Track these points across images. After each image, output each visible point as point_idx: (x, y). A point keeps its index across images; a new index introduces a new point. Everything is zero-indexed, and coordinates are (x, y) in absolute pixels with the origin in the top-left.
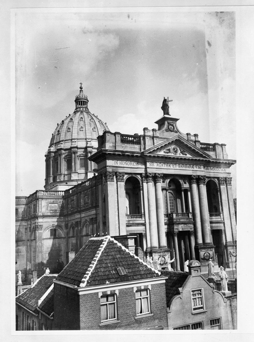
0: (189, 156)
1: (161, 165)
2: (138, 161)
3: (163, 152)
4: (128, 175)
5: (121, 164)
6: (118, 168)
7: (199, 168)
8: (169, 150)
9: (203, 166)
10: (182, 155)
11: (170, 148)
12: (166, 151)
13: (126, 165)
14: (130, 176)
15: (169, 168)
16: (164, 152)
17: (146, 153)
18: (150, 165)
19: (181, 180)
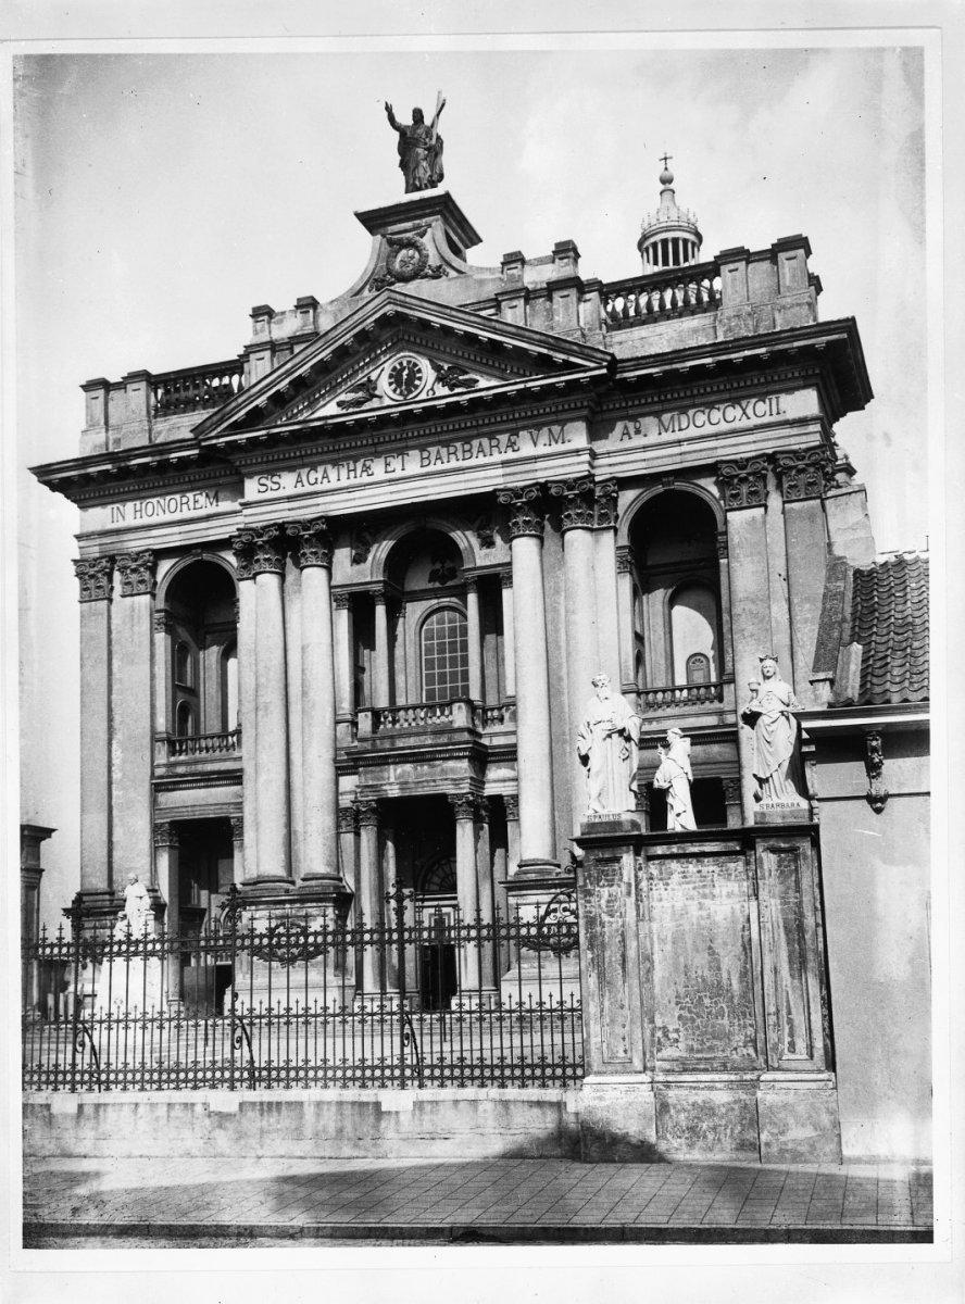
0: (486, 384)
1: (319, 475)
2: (215, 486)
3: (334, 403)
4: (173, 561)
5: (138, 514)
6: (125, 537)
7: (554, 439)
8: (369, 388)
9: (581, 426)
10: (442, 390)
11: (373, 376)
12: (351, 396)
13: (161, 511)
14: (189, 561)
15: (366, 479)
16: (339, 404)
17: (213, 434)
18: (264, 488)
19: (464, 528)
